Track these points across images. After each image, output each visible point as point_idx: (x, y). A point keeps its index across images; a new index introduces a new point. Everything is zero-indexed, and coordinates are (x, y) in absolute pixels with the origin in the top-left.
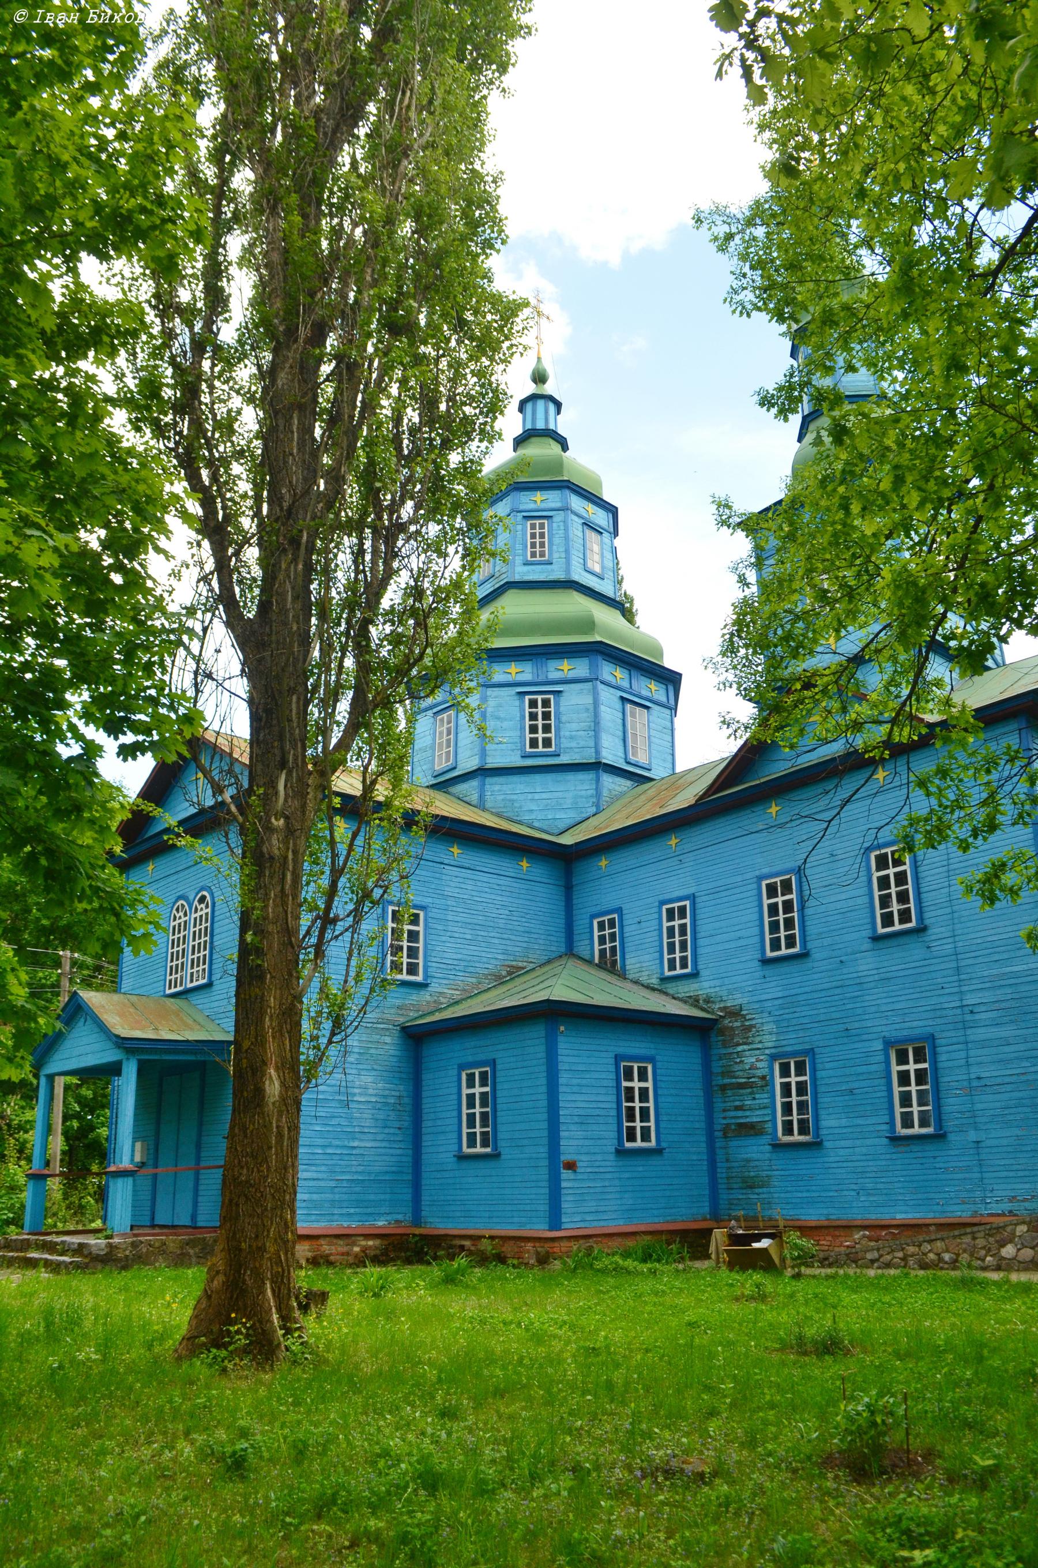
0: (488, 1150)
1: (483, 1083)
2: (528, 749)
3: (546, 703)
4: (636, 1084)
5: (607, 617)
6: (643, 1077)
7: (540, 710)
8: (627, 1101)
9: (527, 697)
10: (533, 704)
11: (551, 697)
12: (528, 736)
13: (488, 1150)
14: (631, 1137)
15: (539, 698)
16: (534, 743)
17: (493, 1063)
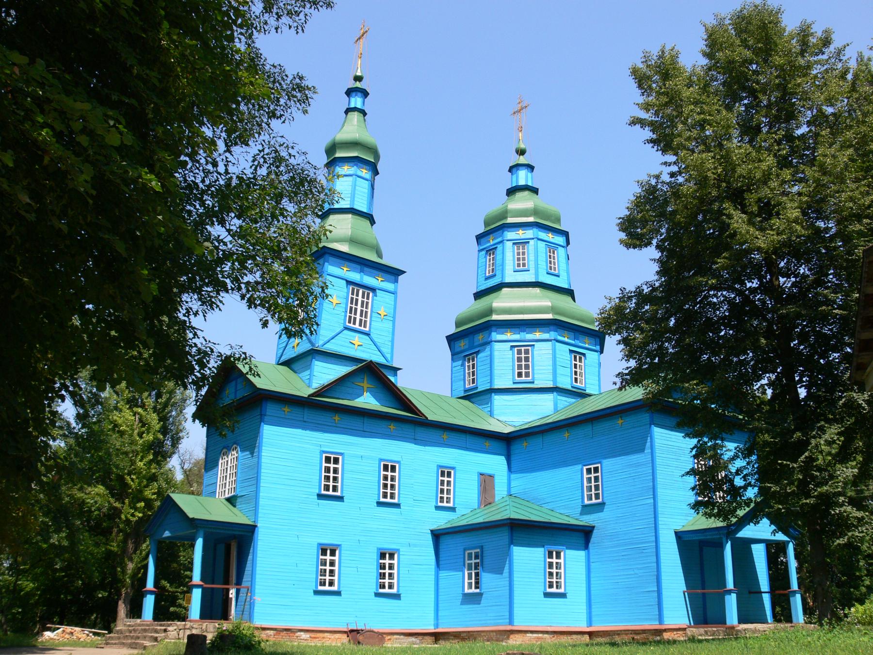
0: (478, 591)
1: (477, 557)
2: (517, 378)
3: (527, 352)
4: (554, 560)
5: (564, 301)
6: (558, 557)
7: (523, 356)
8: (549, 568)
9: (516, 349)
10: (519, 352)
11: (530, 348)
12: (517, 371)
13: (478, 591)
14: (551, 586)
15: (523, 349)
16: (520, 375)
17: (482, 548)
